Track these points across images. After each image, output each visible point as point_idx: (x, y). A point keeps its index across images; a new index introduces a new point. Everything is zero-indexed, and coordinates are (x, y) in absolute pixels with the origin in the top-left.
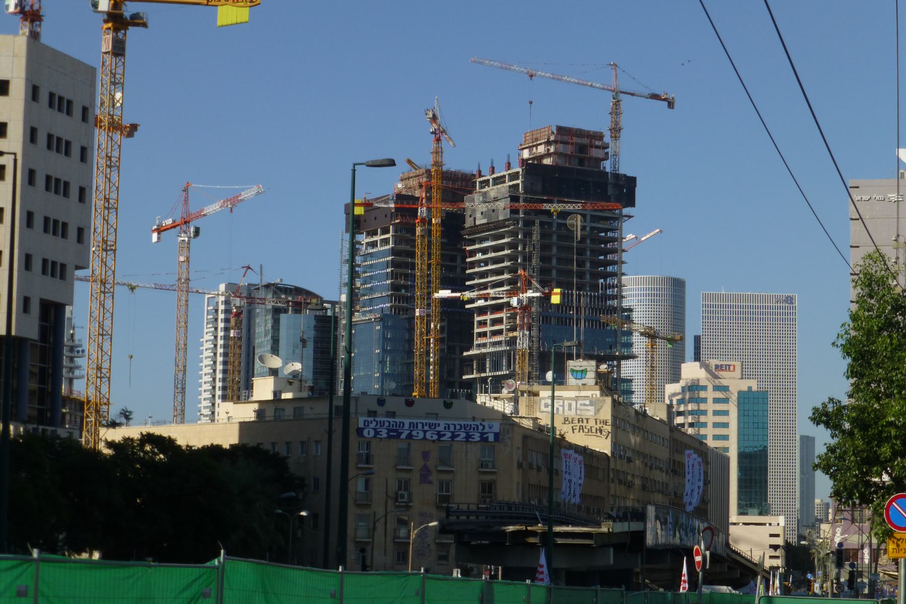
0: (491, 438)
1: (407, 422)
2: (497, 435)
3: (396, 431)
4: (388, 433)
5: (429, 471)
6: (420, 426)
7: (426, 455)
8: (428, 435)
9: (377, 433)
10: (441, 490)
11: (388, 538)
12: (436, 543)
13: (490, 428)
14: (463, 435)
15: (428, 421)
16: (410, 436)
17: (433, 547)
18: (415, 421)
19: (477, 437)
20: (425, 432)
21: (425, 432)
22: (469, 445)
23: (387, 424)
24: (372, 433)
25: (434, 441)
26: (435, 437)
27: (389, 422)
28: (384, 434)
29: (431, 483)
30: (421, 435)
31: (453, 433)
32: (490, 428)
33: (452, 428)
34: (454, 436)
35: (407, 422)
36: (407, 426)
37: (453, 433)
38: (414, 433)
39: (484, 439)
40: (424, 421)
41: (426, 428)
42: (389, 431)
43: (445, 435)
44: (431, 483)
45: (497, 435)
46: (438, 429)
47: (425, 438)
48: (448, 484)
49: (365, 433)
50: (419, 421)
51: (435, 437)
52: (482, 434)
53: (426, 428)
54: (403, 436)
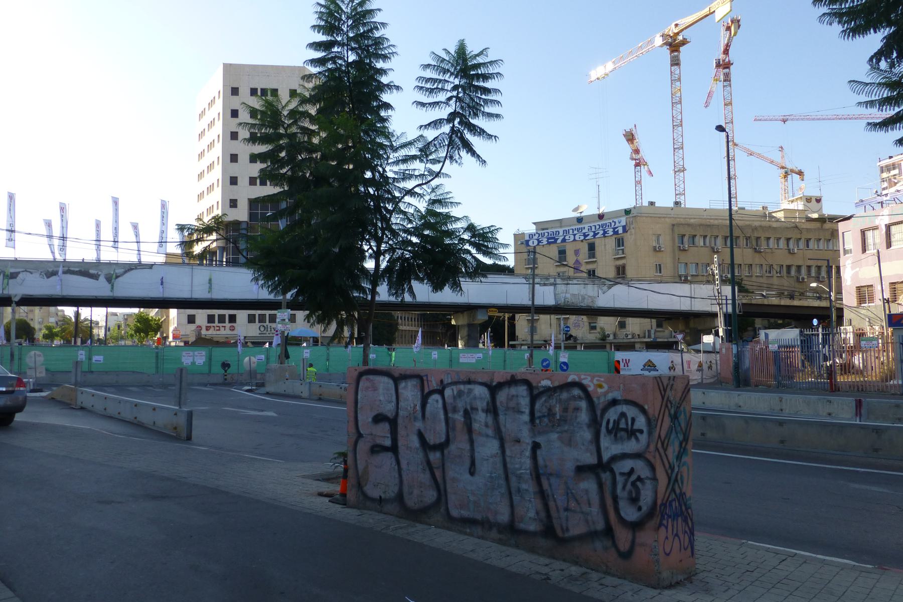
0: (620, 230)
1: (561, 231)
2: (624, 227)
3: (553, 238)
7: (577, 252)
8: (577, 238)
9: (539, 242)
14: (601, 232)
16: (564, 240)
19: (611, 232)
20: (575, 235)
21: (575, 235)
22: (607, 240)
24: (536, 242)
26: (582, 238)
28: (545, 241)
30: (572, 238)
33: (593, 229)
34: (595, 234)
35: (561, 231)
36: (561, 233)
38: (567, 238)
39: (616, 233)
40: (574, 228)
41: (576, 232)
42: (548, 239)
45: (624, 227)
47: (575, 240)
48: (594, 271)
49: (531, 243)
51: (582, 238)
52: (614, 229)
53: (576, 232)
54: (559, 241)
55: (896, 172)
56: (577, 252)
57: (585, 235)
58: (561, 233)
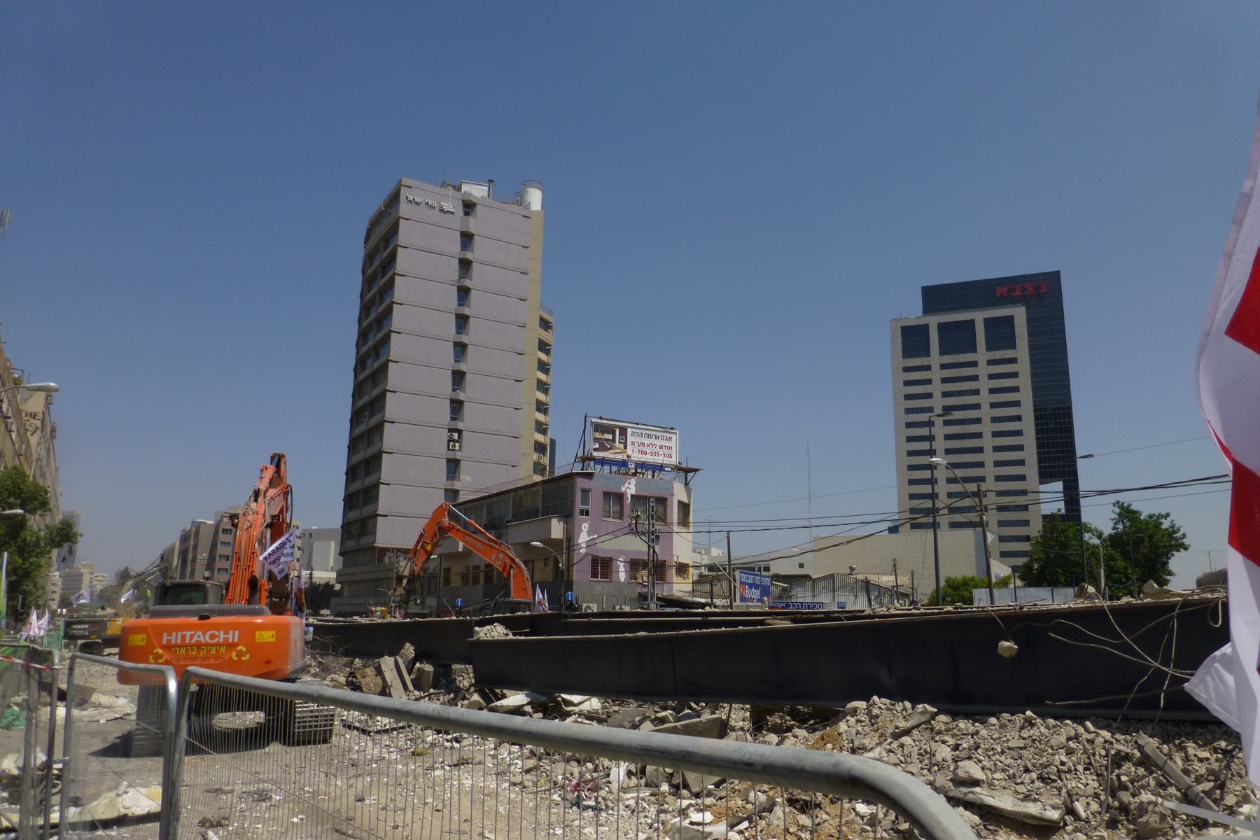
55: (610, 437)
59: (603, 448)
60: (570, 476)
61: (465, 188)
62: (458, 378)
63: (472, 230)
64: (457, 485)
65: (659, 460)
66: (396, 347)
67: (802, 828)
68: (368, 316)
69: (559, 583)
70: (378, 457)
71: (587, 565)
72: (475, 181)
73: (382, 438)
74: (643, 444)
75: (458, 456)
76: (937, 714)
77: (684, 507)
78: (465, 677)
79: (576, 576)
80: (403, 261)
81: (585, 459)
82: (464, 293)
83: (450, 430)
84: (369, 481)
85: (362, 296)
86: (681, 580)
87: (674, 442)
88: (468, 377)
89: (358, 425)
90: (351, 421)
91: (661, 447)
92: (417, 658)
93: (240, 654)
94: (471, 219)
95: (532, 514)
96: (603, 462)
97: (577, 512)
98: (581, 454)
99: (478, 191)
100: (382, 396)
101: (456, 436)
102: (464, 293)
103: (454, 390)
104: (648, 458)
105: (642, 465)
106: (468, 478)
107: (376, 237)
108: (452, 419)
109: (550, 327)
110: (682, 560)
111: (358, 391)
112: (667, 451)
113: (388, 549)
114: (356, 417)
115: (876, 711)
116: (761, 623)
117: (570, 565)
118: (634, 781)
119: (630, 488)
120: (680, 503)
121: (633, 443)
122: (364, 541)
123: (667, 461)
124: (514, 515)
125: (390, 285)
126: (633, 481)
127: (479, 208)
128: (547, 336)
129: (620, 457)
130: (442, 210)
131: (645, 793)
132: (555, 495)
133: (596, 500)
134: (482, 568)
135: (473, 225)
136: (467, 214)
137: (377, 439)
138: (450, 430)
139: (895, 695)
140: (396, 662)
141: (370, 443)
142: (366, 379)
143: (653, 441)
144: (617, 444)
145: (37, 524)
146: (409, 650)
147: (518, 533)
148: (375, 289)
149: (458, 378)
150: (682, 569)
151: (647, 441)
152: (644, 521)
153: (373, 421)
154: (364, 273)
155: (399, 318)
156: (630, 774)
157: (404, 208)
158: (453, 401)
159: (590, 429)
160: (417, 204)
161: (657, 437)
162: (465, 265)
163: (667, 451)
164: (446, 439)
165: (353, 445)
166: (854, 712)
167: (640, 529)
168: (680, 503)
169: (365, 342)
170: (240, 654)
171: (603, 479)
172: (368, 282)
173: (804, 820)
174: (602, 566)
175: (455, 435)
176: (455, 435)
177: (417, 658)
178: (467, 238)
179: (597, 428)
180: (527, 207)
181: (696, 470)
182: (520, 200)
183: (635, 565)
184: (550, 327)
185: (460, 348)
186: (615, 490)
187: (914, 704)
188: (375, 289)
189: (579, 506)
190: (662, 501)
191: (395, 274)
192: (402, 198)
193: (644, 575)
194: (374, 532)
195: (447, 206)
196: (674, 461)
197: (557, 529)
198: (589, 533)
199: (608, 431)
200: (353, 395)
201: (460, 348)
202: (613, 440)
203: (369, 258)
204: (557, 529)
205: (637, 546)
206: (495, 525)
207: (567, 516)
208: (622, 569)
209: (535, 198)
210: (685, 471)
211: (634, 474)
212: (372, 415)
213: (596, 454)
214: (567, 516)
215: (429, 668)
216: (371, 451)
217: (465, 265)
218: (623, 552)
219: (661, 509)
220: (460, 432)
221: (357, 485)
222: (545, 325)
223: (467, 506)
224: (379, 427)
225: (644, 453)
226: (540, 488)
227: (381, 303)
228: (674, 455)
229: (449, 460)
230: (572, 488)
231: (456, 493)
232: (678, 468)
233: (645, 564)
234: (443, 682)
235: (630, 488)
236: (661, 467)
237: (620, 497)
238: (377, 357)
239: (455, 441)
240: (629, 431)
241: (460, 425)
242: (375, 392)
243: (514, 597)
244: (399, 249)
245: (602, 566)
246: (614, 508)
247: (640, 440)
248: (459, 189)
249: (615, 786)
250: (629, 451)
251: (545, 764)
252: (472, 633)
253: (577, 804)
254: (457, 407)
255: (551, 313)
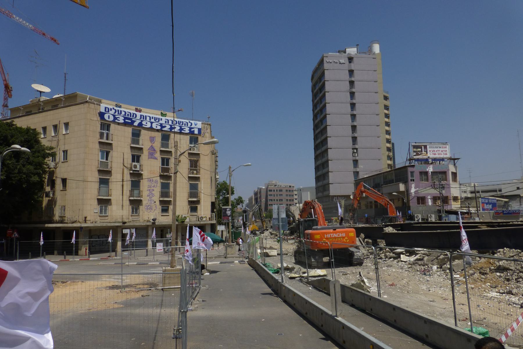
0: (196, 132)
4: (124, 120)
5: (155, 150)
6: (148, 119)
9: (115, 118)
10: (163, 164)
11: (125, 197)
12: (160, 201)
13: (196, 125)
15: (154, 116)
16: (140, 124)
17: (158, 203)
18: (145, 114)
19: (187, 130)
20: (152, 123)
21: (152, 123)
23: (123, 113)
24: (112, 118)
25: (158, 131)
26: (159, 128)
27: (125, 112)
29: (156, 159)
31: (171, 126)
32: (196, 125)
34: (171, 128)
36: (138, 117)
37: (171, 126)
38: (144, 123)
39: (191, 132)
40: (151, 116)
41: (153, 120)
42: (125, 118)
43: (165, 127)
44: (156, 159)
45: (200, 130)
46: (161, 122)
49: (106, 117)
50: (147, 115)
51: (159, 128)
52: (190, 128)
54: (136, 124)
55: (420, 150)
56: (152, 139)
57: (161, 125)
58: (138, 117)
59: (417, 154)
60: (405, 167)
61: (348, 50)
62: (354, 128)
63: (353, 69)
64: (358, 170)
65: (442, 156)
66: (329, 120)
67: (483, 278)
68: (316, 109)
69: (404, 208)
70: (327, 161)
71: (415, 200)
72: (351, 46)
73: (327, 155)
74: (434, 151)
75: (357, 158)
76: (520, 253)
77: (454, 175)
78: (382, 244)
79: (411, 205)
80: (328, 86)
81: (410, 160)
82: (352, 94)
83: (353, 149)
84: (325, 171)
85: (313, 101)
86: (455, 203)
87: (448, 148)
88: (358, 128)
89: (317, 150)
90: (315, 149)
91: (442, 151)
92: (365, 238)
93: (346, 240)
94: (352, 64)
95: (391, 182)
96: (418, 160)
97: (409, 180)
98: (408, 158)
99: (352, 51)
100: (326, 139)
101: (355, 151)
102: (352, 94)
103: (353, 133)
104: (437, 156)
105: (435, 160)
106: (362, 167)
107: (316, 78)
108: (353, 144)
109: (388, 99)
110: (455, 195)
111: (316, 138)
112: (445, 152)
113: (335, 196)
114: (316, 148)
115: (505, 252)
116: (476, 227)
117: (408, 201)
118: (439, 269)
119: (430, 169)
120: (452, 173)
121: (430, 151)
122: (326, 193)
123: (445, 156)
124: (384, 182)
125: (324, 95)
126: (431, 166)
127: (355, 59)
128: (387, 103)
129: (425, 157)
130: (340, 63)
131: (443, 272)
132: (400, 175)
133: (417, 175)
134: (373, 202)
135: (353, 66)
136: (350, 62)
137: (326, 155)
138: (353, 149)
139: (511, 248)
140: (359, 240)
141: (323, 157)
142: (319, 133)
143: (439, 149)
144: (423, 152)
145: (232, 198)
146: (362, 235)
147: (386, 189)
148: (318, 98)
149: (354, 128)
150: (455, 199)
151: (436, 149)
152: (437, 183)
153: (324, 149)
154: (312, 92)
155: (329, 109)
156: (438, 268)
157: (326, 66)
158: (353, 137)
159: (411, 148)
160: (331, 63)
161: (440, 147)
162: (352, 83)
163: (445, 152)
164: (352, 152)
165: (316, 158)
166: (499, 252)
167: (436, 187)
168: (452, 173)
169: (317, 119)
170: (346, 240)
171: (419, 168)
172: (315, 96)
173: (483, 276)
174: (421, 200)
175: (355, 150)
176: (355, 150)
177: (365, 238)
178: (351, 72)
179: (415, 147)
180: (374, 54)
181: (458, 159)
182: (370, 50)
183: (435, 199)
184: (388, 99)
185: (353, 117)
186: (424, 171)
187: (516, 249)
188: (318, 98)
189: (410, 178)
190: (445, 173)
191: (325, 92)
192: (325, 62)
193: (439, 202)
194: (329, 190)
195: (342, 61)
196: (448, 156)
197: (402, 187)
198: (415, 188)
199: (419, 148)
200: (314, 139)
201: (353, 117)
202: (422, 151)
203: (314, 87)
204: (402, 187)
205: (435, 192)
206: (377, 186)
207: (405, 182)
208: (430, 201)
209: (376, 48)
210: (453, 160)
211: (432, 163)
212: (323, 146)
213: (415, 157)
214: (405, 182)
215: (370, 241)
216: (324, 160)
217: (352, 83)
218: (429, 194)
219: (444, 176)
220: (357, 149)
221: (320, 173)
222: (386, 98)
223: (365, 180)
224: (326, 151)
225: (435, 154)
226: (393, 172)
227: (321, 103)
228: (448, 154)
229: (354, 161)
230: (406, 172)
231: (358, 172)
232: (451, 159)
233: (439, 198)
234: (375, 244)
235: (430, 169)
236: (443, 159)
237: (426, 173)
238: (322, 124)
239: (355, 153)
240: (428, 146)
241: (357, 146)
242: (323, 138)
243: (390, 215)
244: (326, 82)
245: (421, 200)
246: (424, 177)
247: (433, 149)
248: (345, 52)
249: (434, 271)
250: (429, 155)
251: (413, 266)
252: (383, 230)
253: (425, 274)
254: (354, 139)
255: (388, 93)
